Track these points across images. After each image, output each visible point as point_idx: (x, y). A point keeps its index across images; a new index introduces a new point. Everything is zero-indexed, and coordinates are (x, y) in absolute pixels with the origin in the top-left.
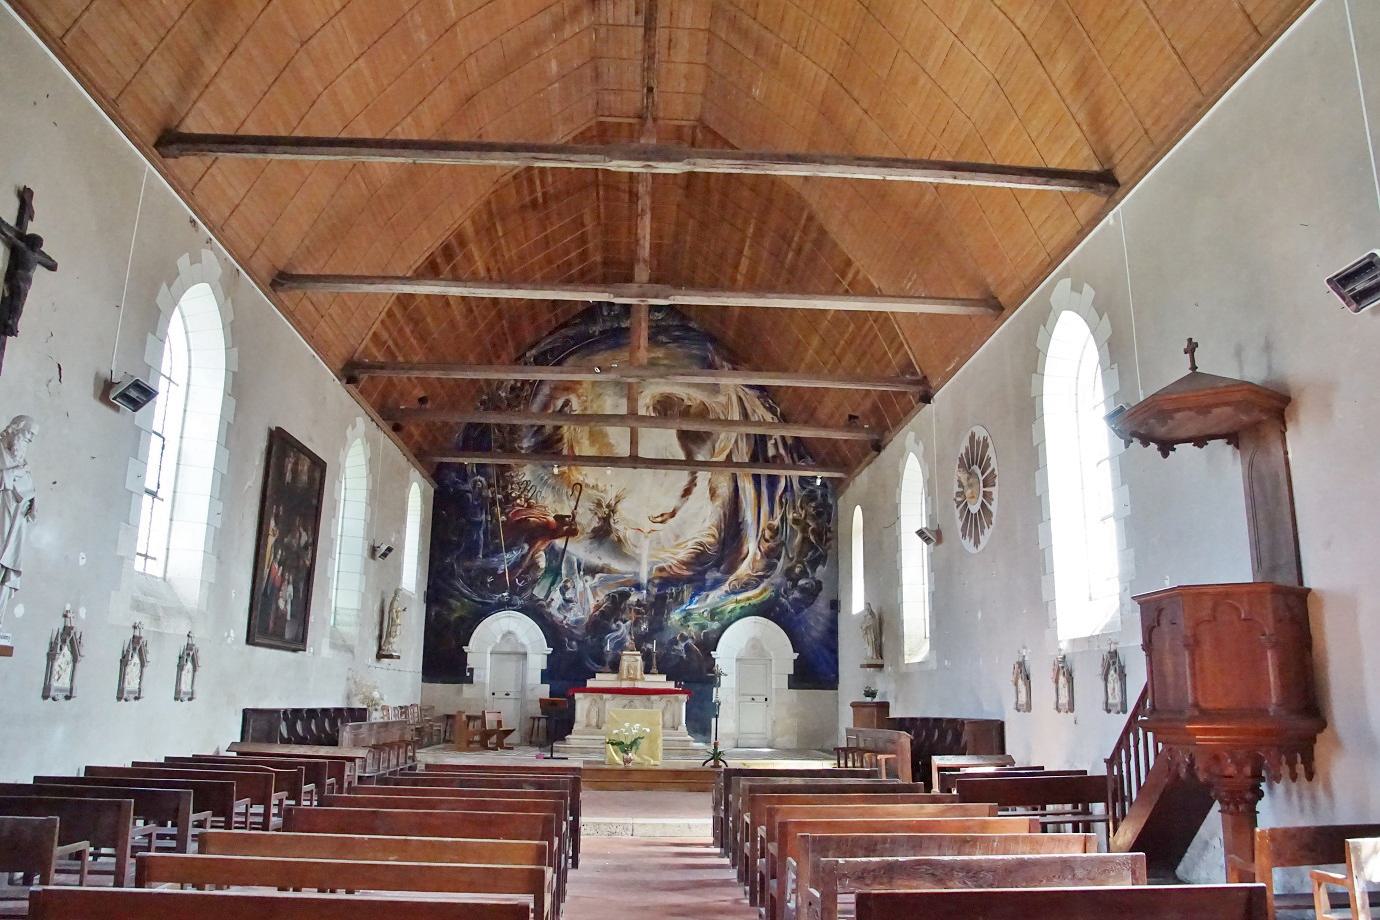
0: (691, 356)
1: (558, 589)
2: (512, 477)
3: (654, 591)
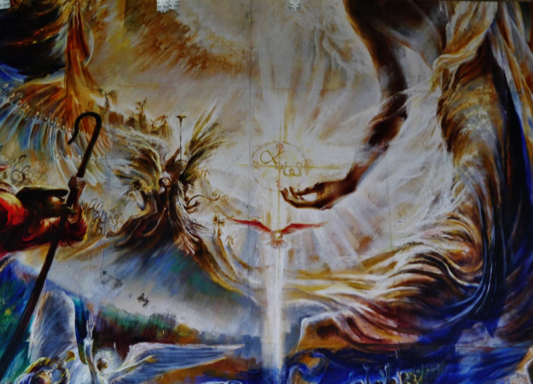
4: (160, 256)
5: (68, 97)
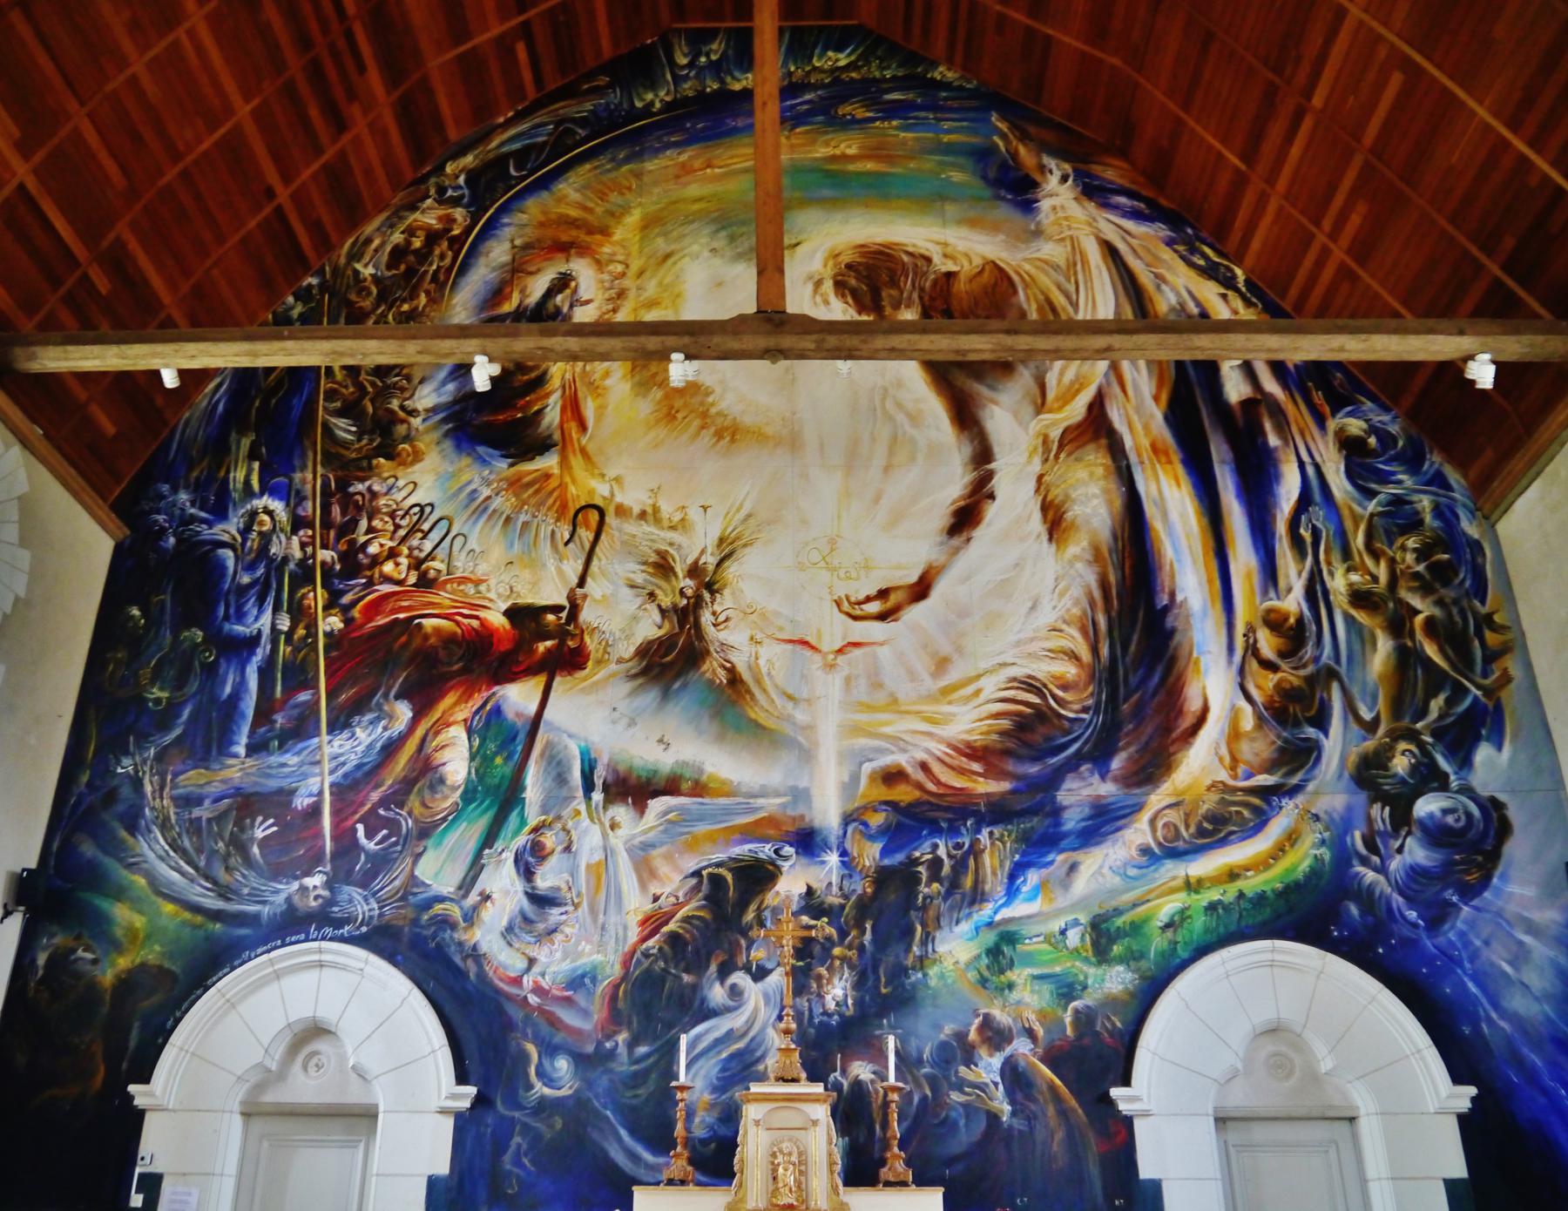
0: (948, 149)
1: (509, 857)
2: (374, 495)
3: (870, 854)
4: (684, 686)
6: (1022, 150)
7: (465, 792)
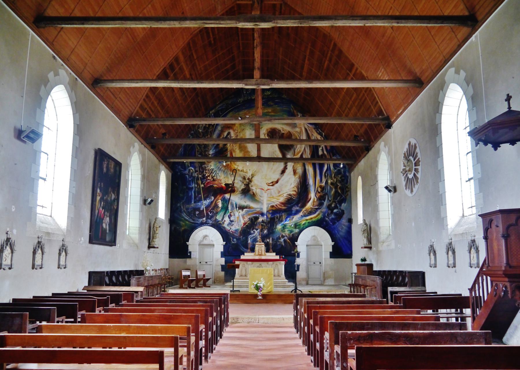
1: (227, 216)
2: (206, 167)
5: (231, 166)
6: (295, 111)
7: (221, 208)
